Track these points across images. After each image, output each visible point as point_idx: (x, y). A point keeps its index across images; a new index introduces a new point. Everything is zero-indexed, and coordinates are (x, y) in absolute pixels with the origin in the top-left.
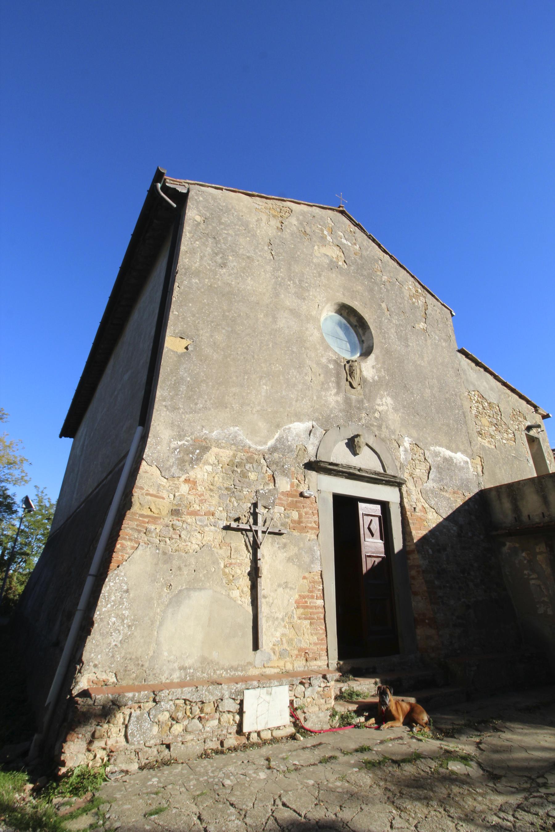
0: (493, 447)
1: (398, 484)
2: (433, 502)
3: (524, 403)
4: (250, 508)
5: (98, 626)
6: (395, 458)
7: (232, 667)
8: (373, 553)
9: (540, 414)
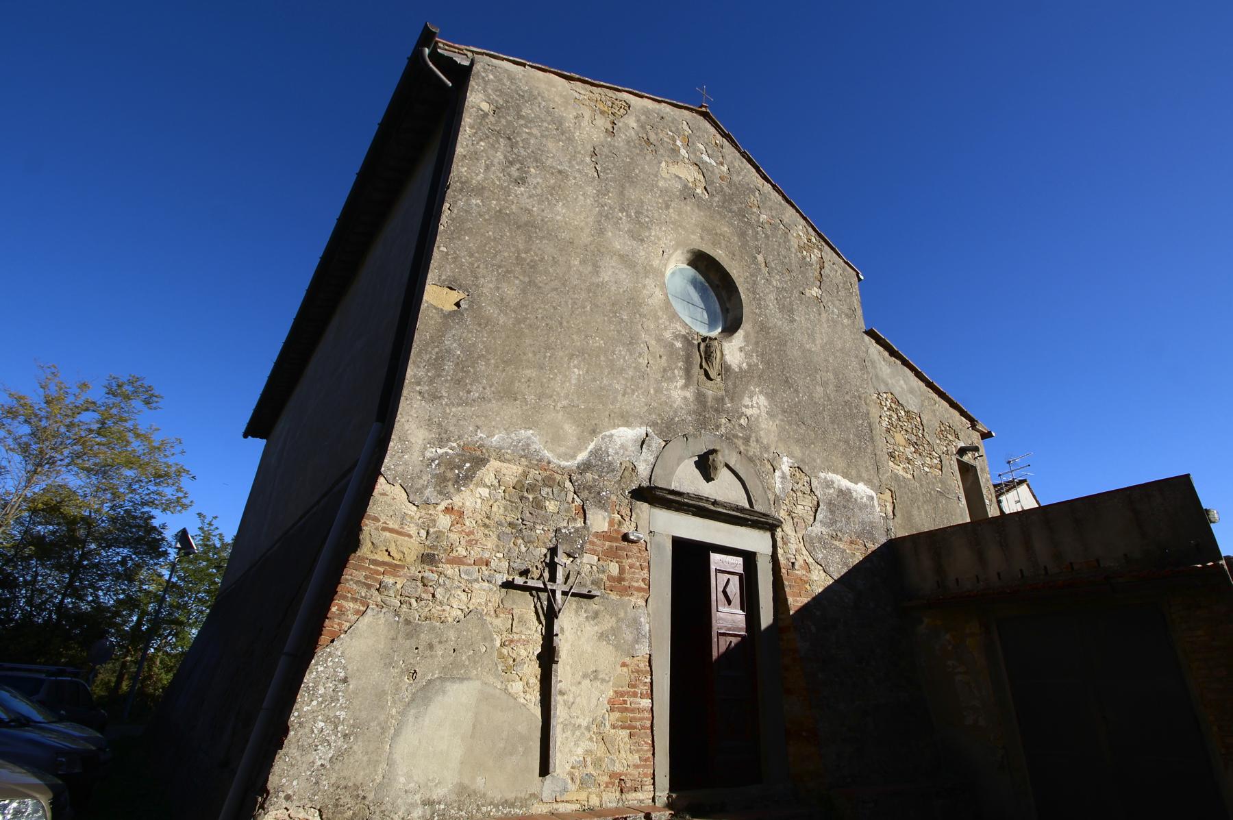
0: (910, 477)
1: (768, 525)
2: (820, 556)
3: (957, 414)
4: (545, 556)
5: (296, 734)
6: (768, 488)
7: (506, 801)
8: (729, 629)
9: (978, 431)
